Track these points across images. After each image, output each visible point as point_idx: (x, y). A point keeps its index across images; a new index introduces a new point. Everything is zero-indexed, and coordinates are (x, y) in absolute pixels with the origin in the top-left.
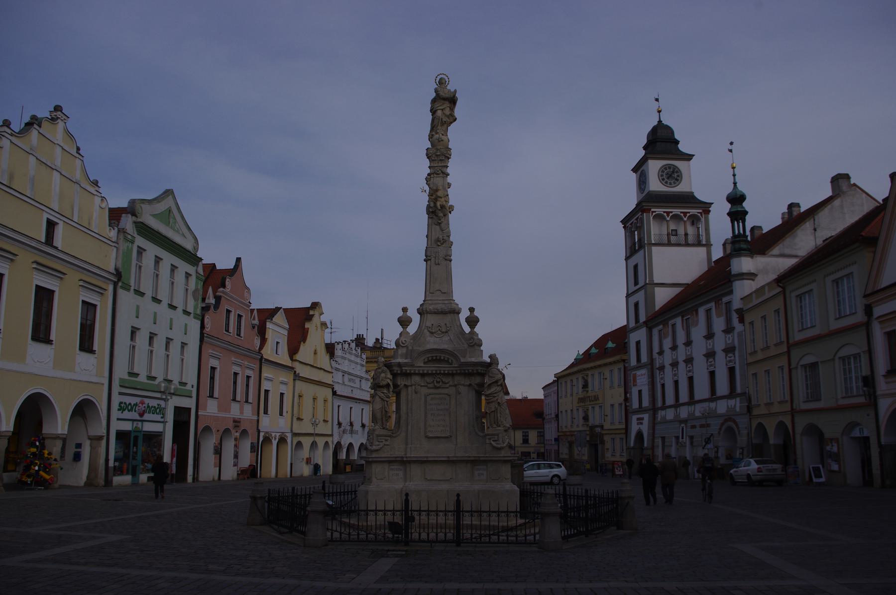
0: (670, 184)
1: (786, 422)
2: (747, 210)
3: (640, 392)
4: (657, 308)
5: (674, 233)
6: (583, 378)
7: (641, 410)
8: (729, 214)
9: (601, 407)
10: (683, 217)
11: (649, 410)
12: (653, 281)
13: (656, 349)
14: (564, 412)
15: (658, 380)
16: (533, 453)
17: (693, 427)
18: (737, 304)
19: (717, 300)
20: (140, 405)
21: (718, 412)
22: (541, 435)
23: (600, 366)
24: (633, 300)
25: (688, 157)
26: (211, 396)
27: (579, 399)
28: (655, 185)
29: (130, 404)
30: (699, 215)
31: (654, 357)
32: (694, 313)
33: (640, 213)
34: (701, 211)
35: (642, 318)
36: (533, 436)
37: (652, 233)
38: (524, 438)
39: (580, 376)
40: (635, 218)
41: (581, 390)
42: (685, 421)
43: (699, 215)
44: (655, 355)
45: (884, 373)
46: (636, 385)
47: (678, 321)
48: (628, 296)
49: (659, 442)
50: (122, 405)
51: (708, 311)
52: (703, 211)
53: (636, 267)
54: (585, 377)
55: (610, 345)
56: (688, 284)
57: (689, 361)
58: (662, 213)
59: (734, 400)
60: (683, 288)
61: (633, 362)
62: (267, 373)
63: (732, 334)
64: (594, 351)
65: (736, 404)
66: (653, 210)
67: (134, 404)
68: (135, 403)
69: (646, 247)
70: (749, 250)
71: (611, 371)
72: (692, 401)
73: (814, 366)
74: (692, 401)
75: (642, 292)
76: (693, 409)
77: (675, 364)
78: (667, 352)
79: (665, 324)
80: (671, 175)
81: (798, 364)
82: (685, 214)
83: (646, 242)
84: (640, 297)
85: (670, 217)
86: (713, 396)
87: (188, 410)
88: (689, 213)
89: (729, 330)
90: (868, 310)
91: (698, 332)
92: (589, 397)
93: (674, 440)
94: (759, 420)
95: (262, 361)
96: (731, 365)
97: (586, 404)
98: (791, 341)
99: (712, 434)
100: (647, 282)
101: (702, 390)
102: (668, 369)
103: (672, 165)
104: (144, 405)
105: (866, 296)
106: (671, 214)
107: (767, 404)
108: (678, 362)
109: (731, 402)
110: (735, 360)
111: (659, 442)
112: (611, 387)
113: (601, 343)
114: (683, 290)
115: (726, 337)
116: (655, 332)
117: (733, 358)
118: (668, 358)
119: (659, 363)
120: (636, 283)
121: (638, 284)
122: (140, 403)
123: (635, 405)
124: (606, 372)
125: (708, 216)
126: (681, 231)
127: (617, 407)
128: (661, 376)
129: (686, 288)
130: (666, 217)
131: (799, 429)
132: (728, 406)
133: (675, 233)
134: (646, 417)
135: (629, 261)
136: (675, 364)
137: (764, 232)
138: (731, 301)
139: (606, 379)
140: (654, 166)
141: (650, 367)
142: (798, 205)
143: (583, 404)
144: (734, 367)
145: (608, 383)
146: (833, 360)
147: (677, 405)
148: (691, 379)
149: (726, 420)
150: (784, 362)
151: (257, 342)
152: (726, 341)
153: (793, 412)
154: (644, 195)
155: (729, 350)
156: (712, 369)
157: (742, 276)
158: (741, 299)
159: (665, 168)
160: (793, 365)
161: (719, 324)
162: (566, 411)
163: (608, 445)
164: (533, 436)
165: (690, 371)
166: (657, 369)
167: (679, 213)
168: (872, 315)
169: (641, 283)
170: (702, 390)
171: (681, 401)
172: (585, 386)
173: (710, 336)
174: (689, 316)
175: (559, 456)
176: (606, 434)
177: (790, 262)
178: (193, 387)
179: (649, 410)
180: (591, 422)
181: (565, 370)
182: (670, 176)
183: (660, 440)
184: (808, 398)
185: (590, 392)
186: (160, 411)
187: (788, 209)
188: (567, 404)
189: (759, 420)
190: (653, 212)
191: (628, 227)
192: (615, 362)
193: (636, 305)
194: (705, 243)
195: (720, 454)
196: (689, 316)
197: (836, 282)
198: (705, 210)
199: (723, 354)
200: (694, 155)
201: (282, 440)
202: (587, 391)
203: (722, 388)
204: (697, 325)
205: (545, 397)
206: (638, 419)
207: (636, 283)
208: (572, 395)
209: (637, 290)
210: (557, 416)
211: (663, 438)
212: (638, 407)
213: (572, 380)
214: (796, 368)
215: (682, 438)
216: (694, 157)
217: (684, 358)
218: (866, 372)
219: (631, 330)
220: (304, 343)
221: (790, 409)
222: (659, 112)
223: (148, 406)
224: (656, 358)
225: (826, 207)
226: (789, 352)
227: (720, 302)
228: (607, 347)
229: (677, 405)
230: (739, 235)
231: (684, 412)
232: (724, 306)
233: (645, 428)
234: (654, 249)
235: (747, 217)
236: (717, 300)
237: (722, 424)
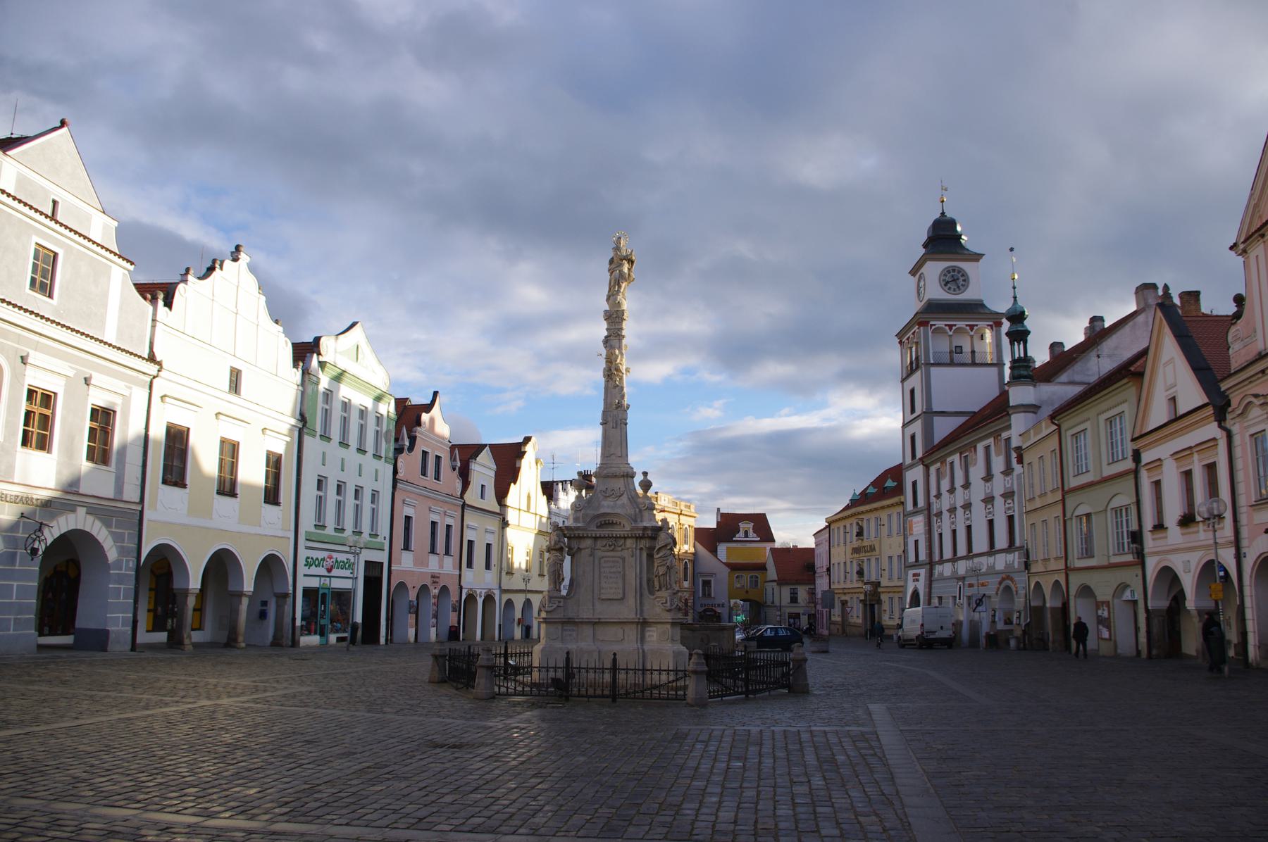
1: (1061, 582)
2: (1029, 329)
3: (916, 542)
4: (936, 442)
5: (958, 350)
6: (858, 524)
7: (917, 564)
9: (877, 559)
11: (926, 564)
12: (932, 409)
13: (933, 492)
14: (836, 565)
15: (936, 529)
16: (804, 614)
17: (971, 586)
18: (1015, 443)
19: (996, 434)
21: (996, 569)
22: (812, 593)
23: (876, 509)
24: (909, 431)
25: (977, 257)
27: (853, 549)
28: (936, 292)
31: (931, 501)
32: (973, 449)
33: (917, 327)
35: (919, 454)
36: (802, 592)
37: (931, 351)
38: (792, 595)
39: (854, 520)
40: (912, 332)
41: (855, 538)
42: (963, 579)
44: (933, 499)
45: (1150, 528)
46: (912, 534)
47: (956, 458)
48: (904, 426)
51: (987, 448)
52: (994, 323)
53: (912, 391)
54: (860, 522)
55: (890, 483)
56: (975, 413)
57: (967, 506)
58: (943, 326)
59: (1013, 555)
60: (967, 418)
61: (910, 507)
62: (470, 519)
63: (1011, 476)
64: (872, 490)
65: (1015, 559)
66: (932, 323)
69: (923, 368)
71: (890, 516)
72: (970, 555)
73: (1088, 515)
74: (970, 555)
76: (992, 562)
77: (952, 510)
78: (945, 495)
79: (943, 461)
80: (954, 279)
81: (1072, 515)
84: (917, 428)
86: (992, 550)
88: (977, 325)
89: (1008, 471)
90: (1137, 456)
91: (977, 472)
92: (864, 547)
93: (951, 600)
94: (1037, 579)
95: (464, 506)
96: (1010, 513)
97: (861, 555)
98: (1066, 488)
99: (984, 595)
101: (980, 544)
102: (946, 515)
103: (958, 267)
105: (1133, 440)
106: (954, 328)
107: (1045, 560)
108: (956, 508)
109: (1010, 557)
110: (1013, 507)
112: (890, 535)
113: (878, 482)
115: (1005, 480)
116: (933, 469)
117: (1011, 505)
118: (946, 502)
119: (937, 509)
120: (913, 411)
121: (914, 412)
123: (912, 558)
124: (883, 515)
125: (1000, 330)
126: (967, 349)
127: (895, 560)
129: (972, 417)
130: (949, 331)
131: (1073, 591)
132: (1006, 561)
133: (959, 349)
134: (923, 572)
135: (905, 383)
136: (952, 510)
137: (1066, 349)
138: (1010, 438)
139: (883, 525)
140: (934, 269)
141: (926, 512)
142: (1101, 319)
143: (858, 555)
144: (1013, 515)
145: (885, 530)
146: (1106, 510)
147: (955, 559)
148: (969, 528)
149: (1003, 579)
150: (1058, 511)
151: (458, 485)
152: (1005, 486)
153: (1067, 571)
154: (923, 303)
155: (1008, 495)
156: (990, 517)
158: (1020, 435)
159: (948, 271)
160: (1068, 515)
161: (998, 464)
162: (839, 564)
163: (886, 606)
164: (802, 592)
165: (968, 519)
167: (964, 326)
168: (1140, 462)
169: (918, 411)
170: (980, 544)
171: (959, 554)
172: (860, 534)
173: (988, 477)
174: (967, 454)
175: (830, 618)
176: (883, 592)
177: (1076, 390)
179: (926, 564)
180: (865, 579)
181: (838, 513)
182: (955, 280)
184: (1082, 554)
185: (865, 540)
187: (1090, 323)
188: (841, 554)
189: (1037, 579)
190: (932, 325)
192: (893, 505)
193: (913, 438)
195: (997, 619)
196: (967, 454)
197: (1110, 421)
199: (1002, 500)
200: (984, 255)
201: (489, 599)
202: (862, 540)
203: (1001, 541)
204: (975, 464)
205: (816, 546)
206: (914, 575)
207: (913, 411)
208: (845, 543)
209: (913, 420)
210: (829, 570)
211: (940, 598)
212: (914, 560)
213: (845, 526)
214: (1071, 519)
215: (960, 599)
216: (984, 257)
217: (962, 504)
218: (1134, 527)
219: (907, 468)
220: (515, 483)
221: (1063, 567)
224: (933, 503)
225: (1127, 324)
226: (1063, 500)
227: (999, 438)
228: (886, 485)
229: (955, 559)
230: (1020, 359)
231: (962, 567)
232: (1003, 443)
233: (921, 586)
234: (933, 370)
235: (1029, 338)
236: (996, 434)
237: (1000, 583)
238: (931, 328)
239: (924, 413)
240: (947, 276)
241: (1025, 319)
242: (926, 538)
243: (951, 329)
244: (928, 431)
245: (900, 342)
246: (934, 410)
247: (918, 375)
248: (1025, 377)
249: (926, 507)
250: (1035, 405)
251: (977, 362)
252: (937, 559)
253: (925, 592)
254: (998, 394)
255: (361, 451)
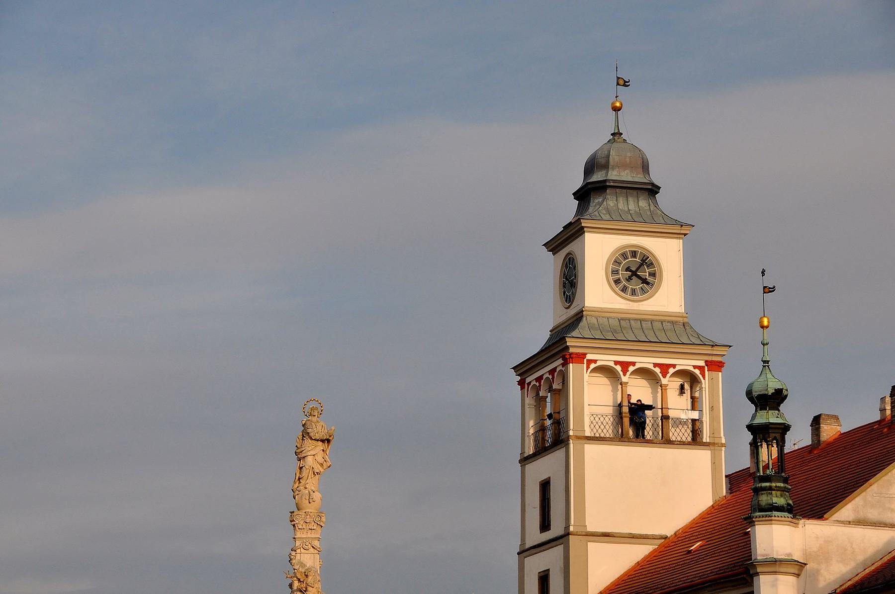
0: (634, 292)
8: (750, 427)
10: (660, 375)
24: (536, 563)
30: (697, 372)
34: (702, 363)
37: (587, 410)
43: (697, 372)
48: (524, 552)
53: (545, 486)
56: (666, 538)
66: (589, 357)
69: (571, 446)
70: (788, 509)
75: (557, 552)
82: (664, 368)
83: (571, 433)
85: (628, 373)
100: (571, 529)
114: (655, 551)
120: (545, 525)
130: (621, 373)
135: (530, 467)
157: (775, 564)
190: (590, 362)
191: (529, 384)
194: (708, 441)
198: (712, 362)
207: (545, 525)
222: (616, 109)
234: (591, 450)
238: (588, 367)
240: (620, 263)
241: (775, 390)
243: (625, 372)
245: (521, 383)
246: (590, 529)
247: (559, 454)
248: (780, 509)
251: (673, 439)
254: (711, 504)
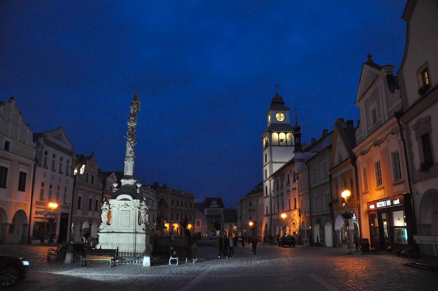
3: (267, 207)
15: (273, 203)
20: (45, 212)
26: (79, 208)
29: (40, 212)
31: (271, 193)
40: (266, 134)
44: (272, 192)
49: (273, 228)
50: (37, 212)
56: (287, 162)
60: (285, 164)
67: (42, 212)
68: (43, 211)
87: (68, 214)
104: (47, 212)
111: (273, 228)
120: (266, 162)
122: (45, 211)
128: (274, 201)
141: (270, 196)
166: (272, 198)
178: (70, 205)
183: (273, 227)
186: (54, 214)
209: (266, 165)
211: (274, 227)
223: (49, 212)
239: (269, 162)
242: (270, 206)
244: (271, 168)
246: (273, 161)
247: (268, 149)
249: (270, 195)
250: (303, 159)
252: (273, 213)
253: (269, 225)
255: (61, 172)
